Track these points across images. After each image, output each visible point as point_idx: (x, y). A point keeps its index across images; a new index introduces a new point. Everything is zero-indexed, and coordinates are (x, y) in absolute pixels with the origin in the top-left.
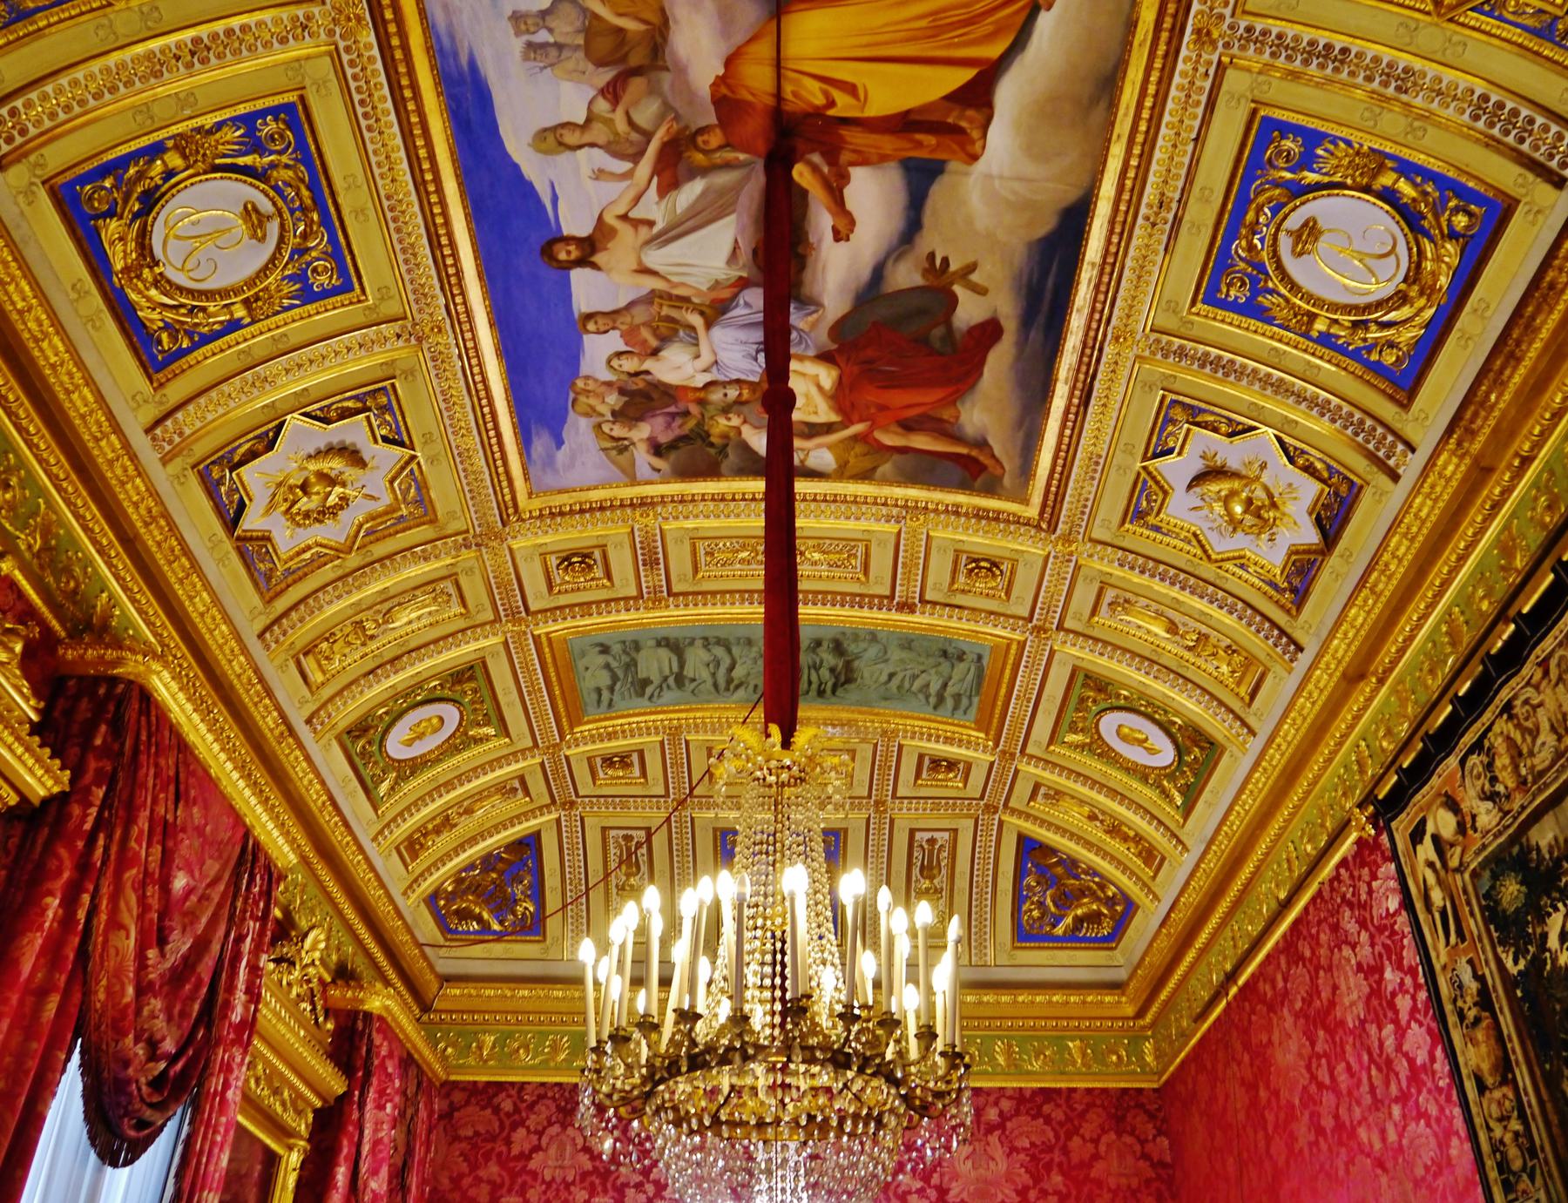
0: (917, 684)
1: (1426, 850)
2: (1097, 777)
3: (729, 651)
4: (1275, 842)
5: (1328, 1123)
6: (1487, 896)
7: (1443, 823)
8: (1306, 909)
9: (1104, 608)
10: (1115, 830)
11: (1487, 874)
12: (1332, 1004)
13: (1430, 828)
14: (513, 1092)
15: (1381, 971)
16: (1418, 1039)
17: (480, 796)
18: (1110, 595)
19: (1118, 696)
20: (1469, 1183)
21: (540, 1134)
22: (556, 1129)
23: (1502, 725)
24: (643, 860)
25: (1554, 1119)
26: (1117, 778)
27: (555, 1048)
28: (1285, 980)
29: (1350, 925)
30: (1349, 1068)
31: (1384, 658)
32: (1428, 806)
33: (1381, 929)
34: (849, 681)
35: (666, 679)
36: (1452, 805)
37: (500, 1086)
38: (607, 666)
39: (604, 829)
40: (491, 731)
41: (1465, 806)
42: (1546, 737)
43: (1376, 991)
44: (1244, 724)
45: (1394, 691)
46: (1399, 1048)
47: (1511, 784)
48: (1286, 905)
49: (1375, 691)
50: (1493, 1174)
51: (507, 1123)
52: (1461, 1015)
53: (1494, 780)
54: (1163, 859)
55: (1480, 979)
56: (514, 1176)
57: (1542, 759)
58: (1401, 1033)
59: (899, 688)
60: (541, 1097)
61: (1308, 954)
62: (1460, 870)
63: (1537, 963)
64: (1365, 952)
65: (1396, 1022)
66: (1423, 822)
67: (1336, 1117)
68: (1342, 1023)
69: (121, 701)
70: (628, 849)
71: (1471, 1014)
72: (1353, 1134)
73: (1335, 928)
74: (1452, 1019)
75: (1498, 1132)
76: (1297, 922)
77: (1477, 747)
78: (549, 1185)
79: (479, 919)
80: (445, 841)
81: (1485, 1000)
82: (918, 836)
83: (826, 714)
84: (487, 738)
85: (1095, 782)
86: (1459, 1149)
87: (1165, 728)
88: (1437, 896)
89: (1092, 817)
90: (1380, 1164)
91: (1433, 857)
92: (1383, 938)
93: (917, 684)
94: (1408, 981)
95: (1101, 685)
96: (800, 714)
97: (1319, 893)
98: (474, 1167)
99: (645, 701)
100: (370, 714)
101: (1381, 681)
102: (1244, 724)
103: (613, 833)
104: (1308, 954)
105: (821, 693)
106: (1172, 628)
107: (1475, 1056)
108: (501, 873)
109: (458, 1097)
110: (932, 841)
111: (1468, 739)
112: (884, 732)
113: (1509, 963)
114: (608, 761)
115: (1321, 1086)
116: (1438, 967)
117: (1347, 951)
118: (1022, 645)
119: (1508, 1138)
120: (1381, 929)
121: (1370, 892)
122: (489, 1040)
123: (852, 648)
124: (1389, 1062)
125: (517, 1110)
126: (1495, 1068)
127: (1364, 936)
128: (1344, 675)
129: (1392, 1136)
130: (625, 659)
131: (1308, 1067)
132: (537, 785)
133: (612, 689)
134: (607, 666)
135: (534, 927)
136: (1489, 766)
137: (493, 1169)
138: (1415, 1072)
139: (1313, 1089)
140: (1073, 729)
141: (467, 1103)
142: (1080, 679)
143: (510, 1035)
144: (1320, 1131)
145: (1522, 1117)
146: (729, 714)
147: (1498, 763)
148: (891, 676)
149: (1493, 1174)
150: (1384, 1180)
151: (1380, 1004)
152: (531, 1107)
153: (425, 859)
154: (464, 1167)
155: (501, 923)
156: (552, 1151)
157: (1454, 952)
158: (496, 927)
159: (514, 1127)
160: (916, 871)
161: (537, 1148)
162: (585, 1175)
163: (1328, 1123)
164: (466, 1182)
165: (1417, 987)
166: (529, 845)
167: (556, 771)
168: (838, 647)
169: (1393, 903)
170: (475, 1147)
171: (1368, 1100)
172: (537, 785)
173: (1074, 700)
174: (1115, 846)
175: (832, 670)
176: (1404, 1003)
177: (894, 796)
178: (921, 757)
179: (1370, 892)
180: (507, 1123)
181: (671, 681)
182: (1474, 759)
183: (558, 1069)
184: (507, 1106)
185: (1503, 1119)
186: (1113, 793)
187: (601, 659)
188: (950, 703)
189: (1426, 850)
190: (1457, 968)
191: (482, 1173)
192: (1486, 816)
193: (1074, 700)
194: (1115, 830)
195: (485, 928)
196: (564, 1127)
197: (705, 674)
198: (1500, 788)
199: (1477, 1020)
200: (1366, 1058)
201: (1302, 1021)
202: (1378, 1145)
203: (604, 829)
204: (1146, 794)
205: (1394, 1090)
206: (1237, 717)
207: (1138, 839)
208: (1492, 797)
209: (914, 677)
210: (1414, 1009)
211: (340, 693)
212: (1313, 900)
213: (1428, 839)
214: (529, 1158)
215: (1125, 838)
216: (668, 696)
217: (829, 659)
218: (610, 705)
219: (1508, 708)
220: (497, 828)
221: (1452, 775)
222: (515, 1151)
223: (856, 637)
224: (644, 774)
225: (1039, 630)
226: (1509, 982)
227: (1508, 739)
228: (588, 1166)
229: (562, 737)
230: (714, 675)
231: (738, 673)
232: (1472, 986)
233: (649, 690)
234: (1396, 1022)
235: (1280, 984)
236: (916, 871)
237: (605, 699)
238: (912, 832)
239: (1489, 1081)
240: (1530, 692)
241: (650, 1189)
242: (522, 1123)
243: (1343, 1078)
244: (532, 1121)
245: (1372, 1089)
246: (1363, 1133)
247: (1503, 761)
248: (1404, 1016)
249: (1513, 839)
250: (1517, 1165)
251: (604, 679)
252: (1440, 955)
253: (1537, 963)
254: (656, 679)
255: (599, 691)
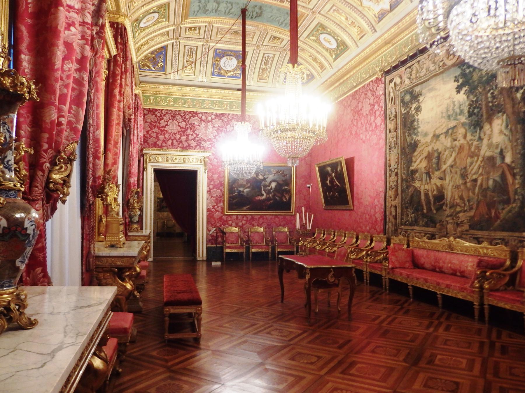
0: (277, 19)
1: (392, 85)
2: (315, 47)
3: (232, 5)
4: (356, 72)
5: (354, 132)
6: (402, 97)
7: (398, 80)
8: (360, 89)
9: (332, 10)
10: (315, 60)
11: (404, 93)
12: (361, 110)
13: (394, 81)
14: (160, 111)
15: (374, 106)
16: (379, 121)
17: (155, 36)
18: (334, 8)
19: (327, 31)
20: (382, 148)
21: (167, 122)
22: (171, 121)
23: (416, 65)
24: (194, 55)
25: (402, 139)
26: (320, 49)
27: (170, 101)
28: (351, 102)
29: (369, 94)
30: (361, 123)
31: (395, 41)
32: (396, 76)
33: (377, 97)
34: (260, 16)
35: (213, 10)
36: (401, 77)
37: (156, 110)
38: (199, 6)
39: (185, 46)
40: (164, 20)
41: (403, 78)
42: (424, 70)
43: (372, 109)
44: (356, 44)
45: (395, 48)
46: (374, 121)
47: (414, 77)
48: (355, 87)
49: (390, 47)
50: (388, 147)
51: (159, 119)
52: (390, 118)
53: (411, 75)
54: (325, 69)
55: (396, 113)
56: (162, 131)
57: (422, 74)
58: (375, 118)
59: (272, 19)
60: (167, 113)
61: (358, 98)
62: (398, 90)
63: (408, 112)
64: (372, 101)
65: (375, 116)
66: (393, 79)
67: (356, 132)
68: (362, 114)
69: (121, 29)
70: (191, 51)
71: (392, 118)
72: (359, 135)
73: (366, 94)
74: (388, 118)
75: (391, 140)
76: (356, 91)
77: (410, 67)
78: (170, 134)
79: (149, 67)
80: (146, 47)
81: (396, 116)
82: (265, 55)
83: (251, 23)
84: (163, 21)
85: (314, 49)
86: (382, 142)
87: (337, 40)
88: (392, 95)
89: (310, 56)
90: (364, 142)
91: (393, 86)
92: (376, 99)
93: (277, 19)
94: (380, 109)
95: (324, 27)
96: (246, 22)
97: (364, 86)
98: (152, 129)
99: (205, 15)
100: (139, 16)
101: (392, 45)
102: (356, 44)
103: (187, 47)
104: (358, 98)
105: (252, 18)
106: (347, 19)
107: (391, 126)
108: (155, 55)
109: (146, 112)
110: (268, 56)
111: (408, 65)
112: (265, 29)
113: (403, 111)
114: (190, 28)
115: (354, 125)
116: (387, 108)
117: (367, 100)
118: (308, 15)
119: (393, 141)
120: (377, 97)
121: (376, 89)
122: (152, 98)
123: (264, 8)
124: (371, 124)
125: (161, 116)
126: (394, 129)
127: (372, 98)
128: (385, 42)
129: (368, 137)
130: (204, 4)
131: (352, 121)
132: (171, 34)
133: (198, 12)
134: (199, 6)
135: (163, 69)
136: (411, 72)
137: (156, 130)
138: (376, 126)
139: (352, 126)
140: (313, 36)
141: (148, 113)
142: (319, 25)
143: (158, 97)
144: (351, 134)
145: (397, 138)
146: (226, 20)
147: (413, 72)
148: (271, 16)
149: (388, 147)
150: (364, 145)
151: (372, 112)
152: (164, 115)
153: (141, 51)
154: (149, 129)
155: (154, 68)
156: (171, 125)
157: (392, 106)
158: (153, 69)
159: (161, 120)
160: (263, 63)
161: (167, 125)
162: (179, 132)
163: (354, 132)
164: (150, 132)
165: (382, 110)
166: (165, 48)
167: (177, 31)
168: (260, 8)
169: (381, 93)
170: (151, 124)
171: (364, 130)
172: (171, 34)
173: (315, 30)
174: (314, 64)
175: (257, 13)
176: (378, 113)
177: (262, 45)
178: (272, 36)
179: (376, 89)
180: (159, 119)
181: (214, 11)
182: (408, 70)
183: (170, 106)
184: (158, 115)
185: (393, 138)
186: (318, 52)
187: (198, 4)
188: (284, 24)
189: (392, 85)
190: (392, 109)
191: (153, 130)
192: (407, 82)
193: (315, 30)
194: (315, 60)
195: (150, 69)
196: (173, 120)
197: (223, 10)
198: (412, 77)
199: (393, 120)
200: (366, 122)
201: (352, 112)
202: (364, 138)
203: (185, 46)
204: (327, 55)
205: (371, 129)
206: (355, 42)
207: (320, 63)
208: (410, 78)
209: (277, 17)
210: (380, 114)
211: (136, 11)
212: (362, 87)
213: (393, 83)
214: (165, 127)
215: (317, 62)
216: (212, 14)
217: (257, 10)
218: (196, 15)
219: (419, 61)
220: (158, 44)
221: (402, 71)
222: (161, 126)
223: (266, 6)
224: (199, 33)
225: (313, 12)
226: (402, 114)
227: (416, 68)
228: (180, 130)
229: (181, 22)
230: (225, 11)
231: (232, 11)
232: (394, 113)
233: (207, 12)
234: (375, 116)
235: (349, 103)
236: (263, 63)
237: (195, 14)
238: (264, 54)
239: (392, 131)
240: (424, 60)
241: (195, 135)
242: (163, 119)
243: (359, 125)
244: (165, 118)
245: (366, 128)
246: (361, 136)
247: (414, 72)
248: (377, 115)
249: (411, 88)
250: (393, 146)
251: (197, 9)
252: (389, 105)
253: (408, 112)
254: (210, 10)
255: (194, 12)
